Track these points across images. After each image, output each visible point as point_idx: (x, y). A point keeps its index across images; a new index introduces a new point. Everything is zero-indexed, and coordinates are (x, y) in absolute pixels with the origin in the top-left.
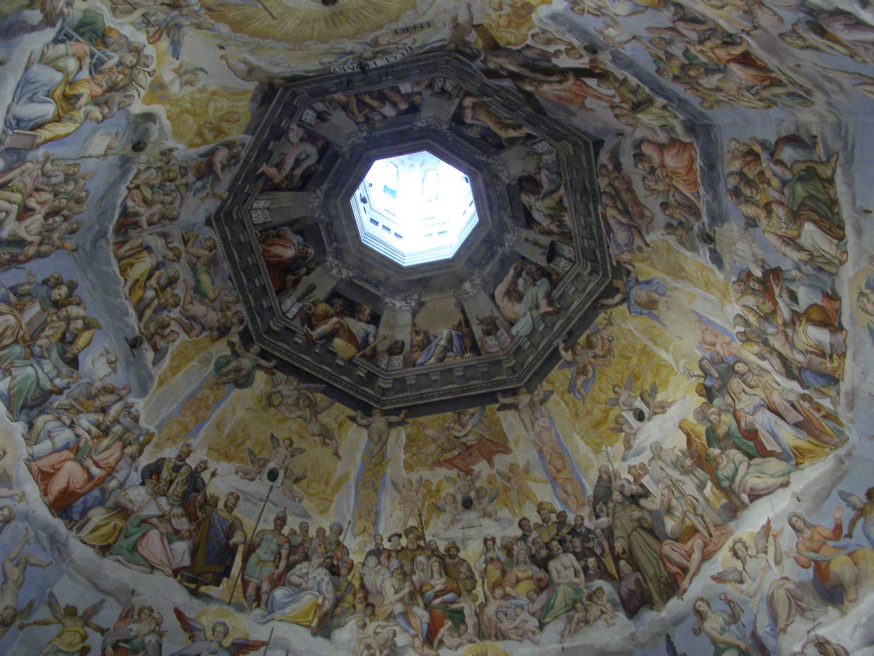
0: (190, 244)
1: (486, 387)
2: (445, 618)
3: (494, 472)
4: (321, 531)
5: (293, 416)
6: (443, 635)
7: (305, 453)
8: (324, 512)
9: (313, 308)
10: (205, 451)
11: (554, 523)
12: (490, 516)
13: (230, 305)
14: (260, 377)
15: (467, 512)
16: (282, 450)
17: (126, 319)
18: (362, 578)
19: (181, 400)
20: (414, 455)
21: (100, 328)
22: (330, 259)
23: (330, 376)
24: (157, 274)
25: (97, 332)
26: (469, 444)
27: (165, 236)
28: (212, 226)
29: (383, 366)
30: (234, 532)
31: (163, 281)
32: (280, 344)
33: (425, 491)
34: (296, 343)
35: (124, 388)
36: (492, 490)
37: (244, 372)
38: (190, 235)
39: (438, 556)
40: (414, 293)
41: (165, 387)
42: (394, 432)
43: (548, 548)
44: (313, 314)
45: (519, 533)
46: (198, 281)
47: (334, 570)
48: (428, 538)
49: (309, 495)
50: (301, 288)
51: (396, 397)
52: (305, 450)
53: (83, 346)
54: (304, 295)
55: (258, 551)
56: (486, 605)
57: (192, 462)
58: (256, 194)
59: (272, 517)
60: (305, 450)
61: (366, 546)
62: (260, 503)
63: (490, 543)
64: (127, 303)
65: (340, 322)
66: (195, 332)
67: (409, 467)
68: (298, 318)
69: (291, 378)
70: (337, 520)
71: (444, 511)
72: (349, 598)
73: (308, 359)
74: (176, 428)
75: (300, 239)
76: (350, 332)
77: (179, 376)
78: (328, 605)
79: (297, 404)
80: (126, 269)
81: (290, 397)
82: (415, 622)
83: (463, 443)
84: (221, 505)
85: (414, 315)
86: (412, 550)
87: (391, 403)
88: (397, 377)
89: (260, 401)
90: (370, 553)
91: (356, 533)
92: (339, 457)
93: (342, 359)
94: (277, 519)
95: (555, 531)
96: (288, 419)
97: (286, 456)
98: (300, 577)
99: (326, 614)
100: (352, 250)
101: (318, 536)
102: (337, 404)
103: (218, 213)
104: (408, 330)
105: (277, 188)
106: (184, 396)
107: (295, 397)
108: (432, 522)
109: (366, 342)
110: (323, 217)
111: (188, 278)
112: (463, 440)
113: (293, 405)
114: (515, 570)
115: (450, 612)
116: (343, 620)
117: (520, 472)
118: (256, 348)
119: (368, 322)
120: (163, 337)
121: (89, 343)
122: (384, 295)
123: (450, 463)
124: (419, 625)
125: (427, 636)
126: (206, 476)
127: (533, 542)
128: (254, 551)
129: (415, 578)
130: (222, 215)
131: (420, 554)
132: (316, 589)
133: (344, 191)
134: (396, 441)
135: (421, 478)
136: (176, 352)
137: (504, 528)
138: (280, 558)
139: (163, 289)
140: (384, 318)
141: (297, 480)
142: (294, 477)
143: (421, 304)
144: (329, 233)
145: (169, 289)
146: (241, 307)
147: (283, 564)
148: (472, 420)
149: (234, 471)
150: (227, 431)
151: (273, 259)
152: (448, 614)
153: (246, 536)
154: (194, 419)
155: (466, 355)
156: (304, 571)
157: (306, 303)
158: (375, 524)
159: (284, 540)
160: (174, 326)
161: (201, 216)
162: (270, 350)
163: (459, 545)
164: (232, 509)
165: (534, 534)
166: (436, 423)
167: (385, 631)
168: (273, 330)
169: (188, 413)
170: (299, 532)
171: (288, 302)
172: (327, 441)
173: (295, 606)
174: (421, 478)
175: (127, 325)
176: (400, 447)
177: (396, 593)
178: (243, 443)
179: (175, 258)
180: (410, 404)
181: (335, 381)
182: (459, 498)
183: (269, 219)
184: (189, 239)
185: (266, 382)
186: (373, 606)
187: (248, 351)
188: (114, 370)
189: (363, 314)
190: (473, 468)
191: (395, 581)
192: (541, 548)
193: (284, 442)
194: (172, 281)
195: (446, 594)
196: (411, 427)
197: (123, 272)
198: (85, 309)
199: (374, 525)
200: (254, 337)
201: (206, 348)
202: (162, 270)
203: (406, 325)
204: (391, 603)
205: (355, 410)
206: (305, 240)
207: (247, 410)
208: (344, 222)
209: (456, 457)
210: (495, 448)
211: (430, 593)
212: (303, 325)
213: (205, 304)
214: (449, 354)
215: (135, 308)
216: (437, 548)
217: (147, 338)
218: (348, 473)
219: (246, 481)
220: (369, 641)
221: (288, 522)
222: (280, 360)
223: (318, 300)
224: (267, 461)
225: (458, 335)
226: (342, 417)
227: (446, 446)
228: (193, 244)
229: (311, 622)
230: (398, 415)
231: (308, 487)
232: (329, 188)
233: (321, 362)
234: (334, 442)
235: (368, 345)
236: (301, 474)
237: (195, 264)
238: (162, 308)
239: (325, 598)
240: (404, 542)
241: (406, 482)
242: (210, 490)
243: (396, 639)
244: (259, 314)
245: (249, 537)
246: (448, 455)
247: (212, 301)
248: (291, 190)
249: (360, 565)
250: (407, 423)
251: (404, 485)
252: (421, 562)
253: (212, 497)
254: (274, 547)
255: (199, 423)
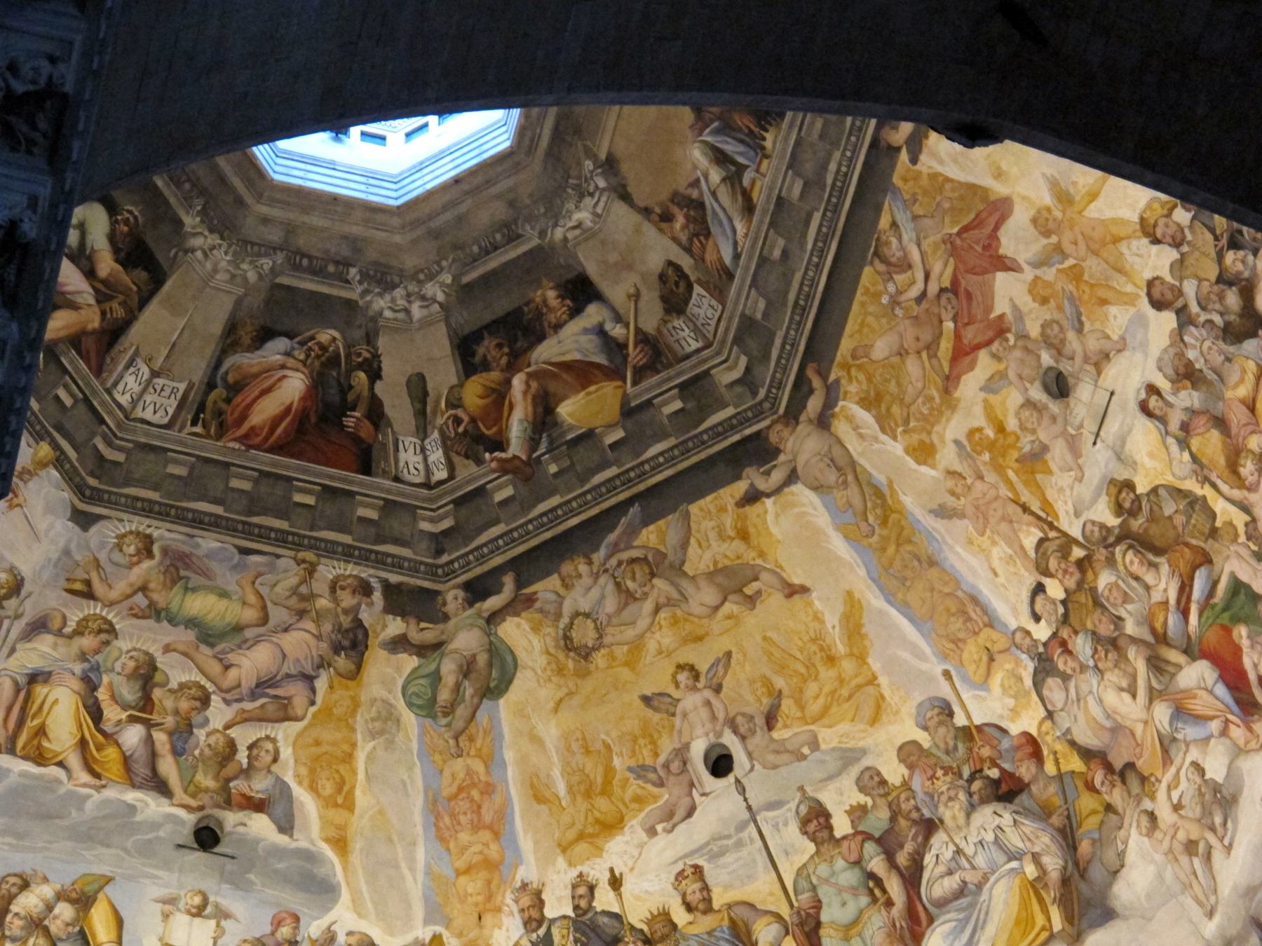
0: (99, 588)
1: (855, 150)
2: (1227, 630)
3: (1029, 274)
4: (909, 753)
5: (643, 623)
6: (1256, 666)
7: (734, 655)
8: (878, 713)
9: (460, 412)
10: (561, 862)
11: (1191, 227)
12: (1107, 356)
13: (304, 589)
14: (514, 631)
15: (1072, 401)
16: (691, 702)
17: (139, 818)
18: (1073, 744)
19: (419, 829)
20: (906, 422)
21: (109, 880)
22: (380, 303)
23: (624, 479)
24: (102, 694)
25: (108, 889)
26: (946, 283)
27: (39, 626)
28: (100, 518)
29: (695, 345)
30: (749, 933)
31: (129, 693)
32: (483, 538)
33: (986, 456)
34: (505, 503)
35: (277, 923)
36: (1060, 308)
37: (482, 659)
38: (81, 575)
39: (1119, 540)
40: (579, 164)
41: (357, 845)
42: (841, 427)
43: (1230, 284)
44: (473, 420)
45: (1168, 320)
46: (192, 623)
47: (1004, 788)
48: (1076, 532)
49: (815, 720)
50: (398, 409)
51: (773, 364)
52: (729, 654)
53: (113, 936)
54: (421, 414)
55: (825, 917)
56: (1254, 520)
57: (558, 906)
58: (95, 382)
59: (793, 829)
60: (729, 654)
61: (1021, 679)
62: (745, 835)
63: (1153, 402)
64: (110, 793)
65: (530, 376)
66: (299, 703)
67: (924, 452)
68: (457, 460)
69: (567, 568)
70: (918, 697)
71: (1045, 448)
72: (1086, 802)
73: (555, 501)
74: (472, 886)
75: (281, 344)
76: (567, 366)
77: (362, 798)
78: (1053, 863)
79: (628, 597)
80: (39, 747)
81: (603, 597)
82: (1202, 704)
83: (938, 296)
84: (680, 917)
85: (625, 197)
86: (1080, 584)
87: (780, 386)
88: (731, 336)
89: (560, 671)
90: (1038, 685)
91: (978, 678)
92: (804, 590)
93: (610, 426)
94: (804, 823)
95: (1209, 237)
96: (642, 636)
97: (708, 703)
98: (950, 873)
99: (1065, 881)
100: (397, 239)
101: (911, 767)
102: (694, 509)
103: (80, 489)
104: (650, 231)
105: (113, 334)
106: (418, 818)
107: (610, 587)
108: (1051, 494)
109: (614, 347)
110: (266, 263)
111: (167, 640)
112: (933, 288)
113: (620, 610)
114: (1229, 394)
115: (1225, 609)
116: (1110, 856)
117: (1058, 214)
118: (453, 597)
119: (576, 312)
120: (247, 772)
121: (120, 923)
122: (542, 234)
123: (963, 354)
124: (1210, 699)
125: (1238, 702)
126: (605, 900)
127: (1203, 308)
128: (818, 924)
129: (1130, 628)
130: (92, 482)
131: (1096, 575)
132: (1001, 858)
133: (237, 182)
134: (861, 436)
135: (957, 442)
136: (304, 771)
137: (1144, 346)
138: (879, 882)
139: (146, 703)
140: (592, 270)
141: (770, 720)
142: (760, 721)
143: (610, 165)
144: (317, 272)
145: (157, 693)
146: (329, 570)
147: (895, 888)
148: (905, 237)
149: (643, 836)
150: (561, 788)
151: (280, 430)
152: (1226, 615)
153: (778, 917)
154: (486, 835)
155: (768, 144)
156: (948, 854)
157: (440, 421)
158: (992, 622)
159: (854, 845)
160: (244, 736)
161: (60, 530)
162: (478, 571)
163: (1123, 475)
164: (708, 900)
165: (1190, 288)
166: (870, 319)
167: (1184, 785)
168: (445, 533)
169: (464, 837)
170: (870, 802)
171: (409, 459)
172: (748, 590)
173: (990, 929)
174: (957, 442)
175: (155, 826)
176: (876, 439)
177: (1134, 696)
178: (609, 771)
179: (104, 636)
180: (802, 348)
181: (642, 476)
182: (1037, 394)
183: (182, 387)
184: (88, 583)
185: (536, 629)
186: (1130, 766)
187: (446, 618)
188: (222, 915)
189: (550, 309)
190: (997, 312)
191: (1113, 677)
192: (1221, 297)
193: (677, 685)
194: (146, 674)
195: (1191, 587)
196: (850, 379)
197: (40, 758)
198: (46, 880)
199: (990, 625)
200: (426, 584)
201: (356, 704)
202: (105, 679)
203: (638, 230)
204: (1146, 723)
205: (738, 477)
206: (290, 336)
207: (556, 710)
208: (316, 220)
209: (958, 336)
210: (988, 230)
211: (1173, 620)
212: (479, 461)
213: (257, 641)
214: (746, 182)
215: (134, 786)
216: (1102, 526)
217: (218, 806)
218: (849, 594)
219: (682, 826)
220: (1181, 835)
221: (830, 807)
222: (514, 564)
223: (452, 388)
224: (682, 753)
225: (716, 132)
226: (728, 521)
227: (927, 337)
228: (104, 580)
229: (1048, 926)
230: (811, 391)
231: (802, 708)
232: (204, 213)
233: (583, 480)
234: (764, 576)
235: (626, 346)
236: (766, 701)
237: (152, 604)
238: (183, 732)
239: (1036, 858)
240: (1055, 590)
241: (950, 483)
242: (637, 916)
243: (1207, 777)
244: (380, 540)
245: (785, 912)
246: (946, 346)
247: (265, 620)
248: (143, 302)
249: (1048, 724)
250: (837, 381)
251: (953, 493)
252: (1112, 587)
253: (649, 922)
254: (850, 877)
255: (499, 828)
